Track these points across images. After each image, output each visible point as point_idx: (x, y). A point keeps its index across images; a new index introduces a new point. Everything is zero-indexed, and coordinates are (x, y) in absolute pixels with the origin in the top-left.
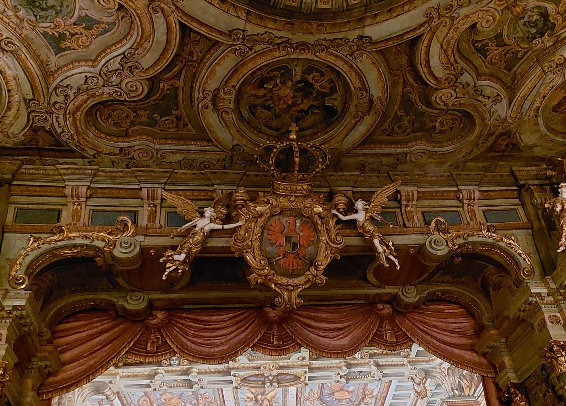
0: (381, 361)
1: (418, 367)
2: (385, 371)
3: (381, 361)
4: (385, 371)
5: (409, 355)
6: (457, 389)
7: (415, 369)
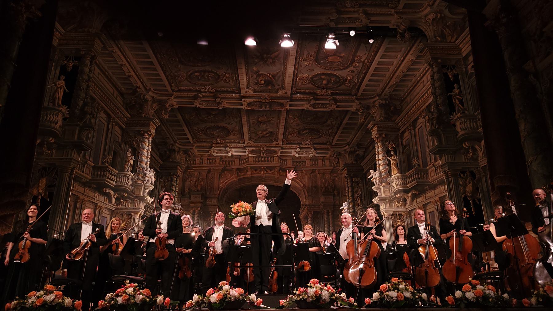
0: (369, 10)
1: (404, 16)
2: (373, 19)
3: (369, 10)
4: (373, 19)
5: (396, 7)
6: (439, 37)
7: (401, 18)
